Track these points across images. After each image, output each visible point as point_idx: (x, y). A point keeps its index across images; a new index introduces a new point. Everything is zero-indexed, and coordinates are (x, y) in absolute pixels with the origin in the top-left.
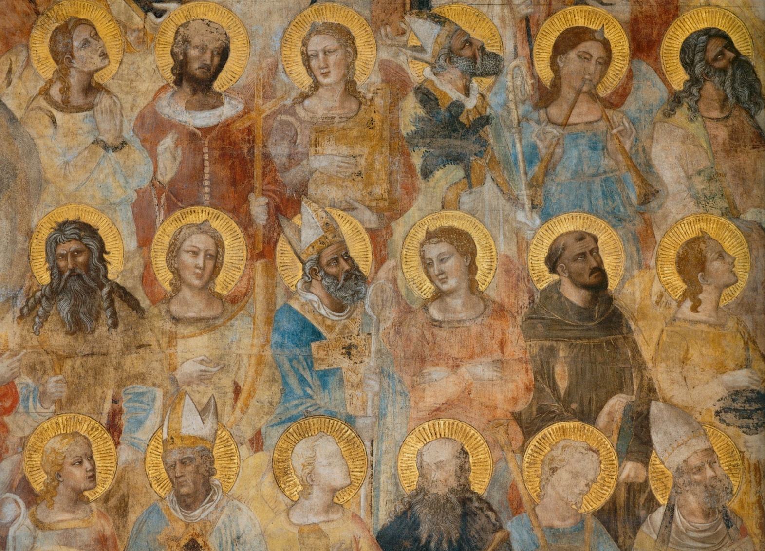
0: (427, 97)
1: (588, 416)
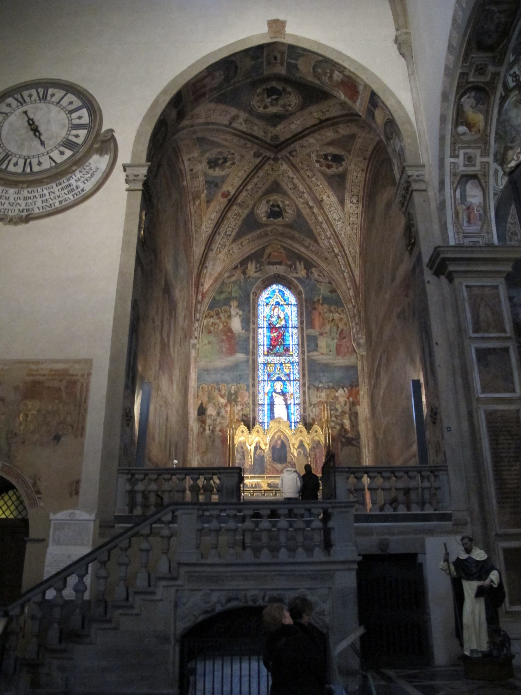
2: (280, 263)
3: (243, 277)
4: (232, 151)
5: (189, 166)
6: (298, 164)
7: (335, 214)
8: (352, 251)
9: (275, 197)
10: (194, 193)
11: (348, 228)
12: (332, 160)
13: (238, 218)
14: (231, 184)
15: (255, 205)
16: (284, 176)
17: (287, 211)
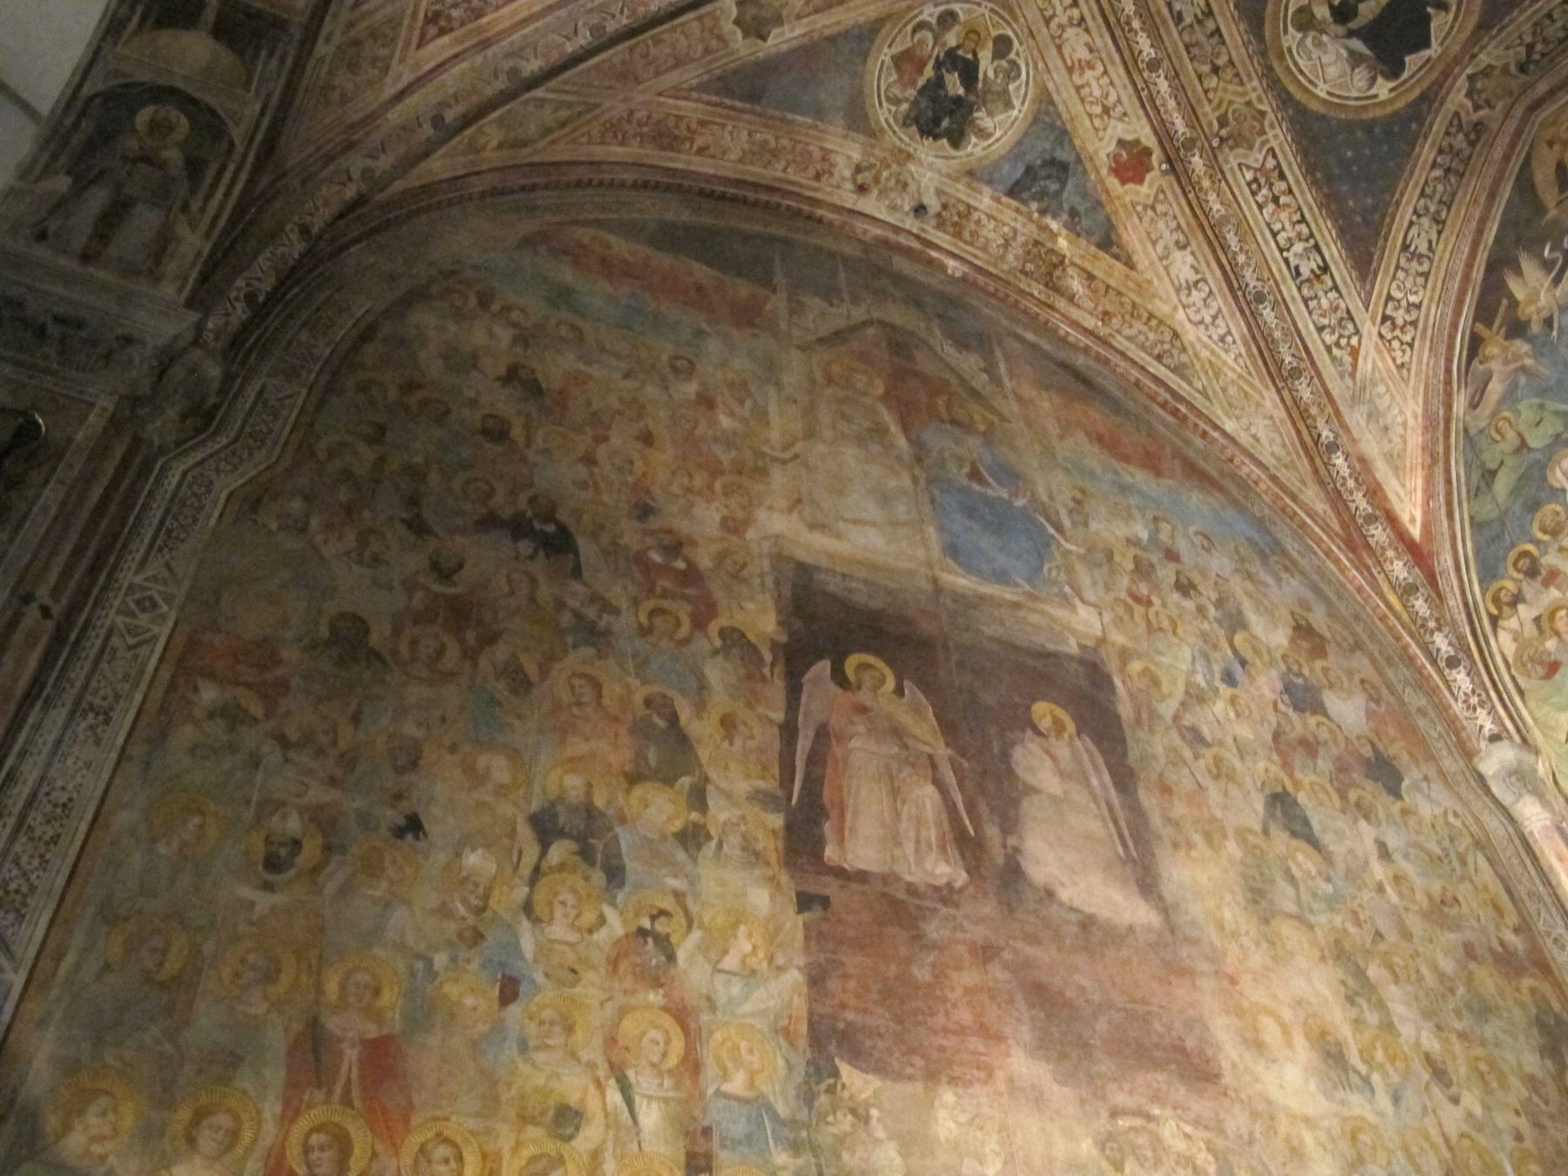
0: (578, 616)
1: (669, 781)
4: (929, 13)
5: (893, 208)
10: (1029, 267)
13: (1280, 186)
14: (1098, 110)
15: (1273, 83)
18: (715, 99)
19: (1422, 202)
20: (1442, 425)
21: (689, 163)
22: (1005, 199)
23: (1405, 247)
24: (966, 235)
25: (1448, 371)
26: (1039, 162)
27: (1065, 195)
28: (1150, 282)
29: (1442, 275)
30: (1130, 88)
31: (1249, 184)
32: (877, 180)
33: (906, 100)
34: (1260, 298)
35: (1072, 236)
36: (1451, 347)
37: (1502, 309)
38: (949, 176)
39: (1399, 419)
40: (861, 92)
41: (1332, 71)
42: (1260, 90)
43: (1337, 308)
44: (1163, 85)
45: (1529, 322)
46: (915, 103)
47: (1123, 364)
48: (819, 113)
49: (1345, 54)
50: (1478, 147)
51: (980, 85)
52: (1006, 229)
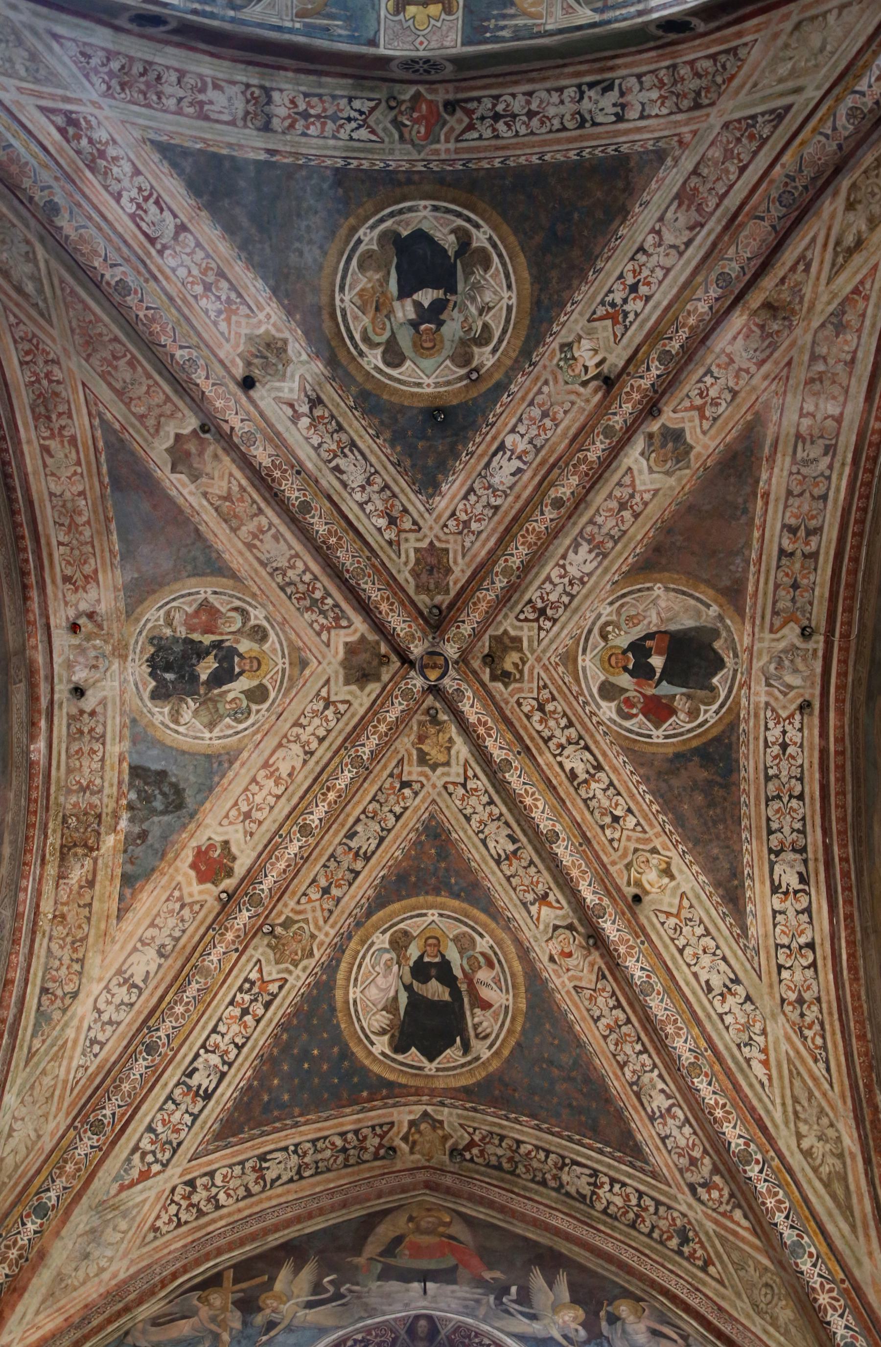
2: (446, 1276)
3: (237, 1325)
4: (257, 616)
6: (528, 717)
7: (706, 960)
8: (820, 1148)
9: (433, 915)
10: (73, 821)
11: (779, 1028)
12: (668, 675)
14: (245, 808)
15: (339, 950)
16: (470, 793)
17: (486, 993)
18: (101, 444)
19: (309, 1145)
20: (120, 1305)
21: (29, 442)
22: (125, 765)
23: (263, 1158)
24: (75, 747)
25: (174, 1276)
26: (174, 780)
27: (156, 819)
28: (113, 941)
29: (257, 1209)
30: (276, 825)
31: (246, 980)
32: (88, 638)
33: (174, 631)
34: (151, 1049)
35: (121, 847)
36: (198, 1262)
37: (258, 1280)
38: (123, 703)
39: (103, 1263)
40: (161, 585)
41: (373, 993)
42: (328, 940)
43: (178, 1131)
44: (293, 848)
45: (260, 1309)
46: (176, 640)
47: (21, 958)
48: (128, 554)
49: (392, 993)
50: (378, 1163)
51: (216, 691)
52: (98, 781)
